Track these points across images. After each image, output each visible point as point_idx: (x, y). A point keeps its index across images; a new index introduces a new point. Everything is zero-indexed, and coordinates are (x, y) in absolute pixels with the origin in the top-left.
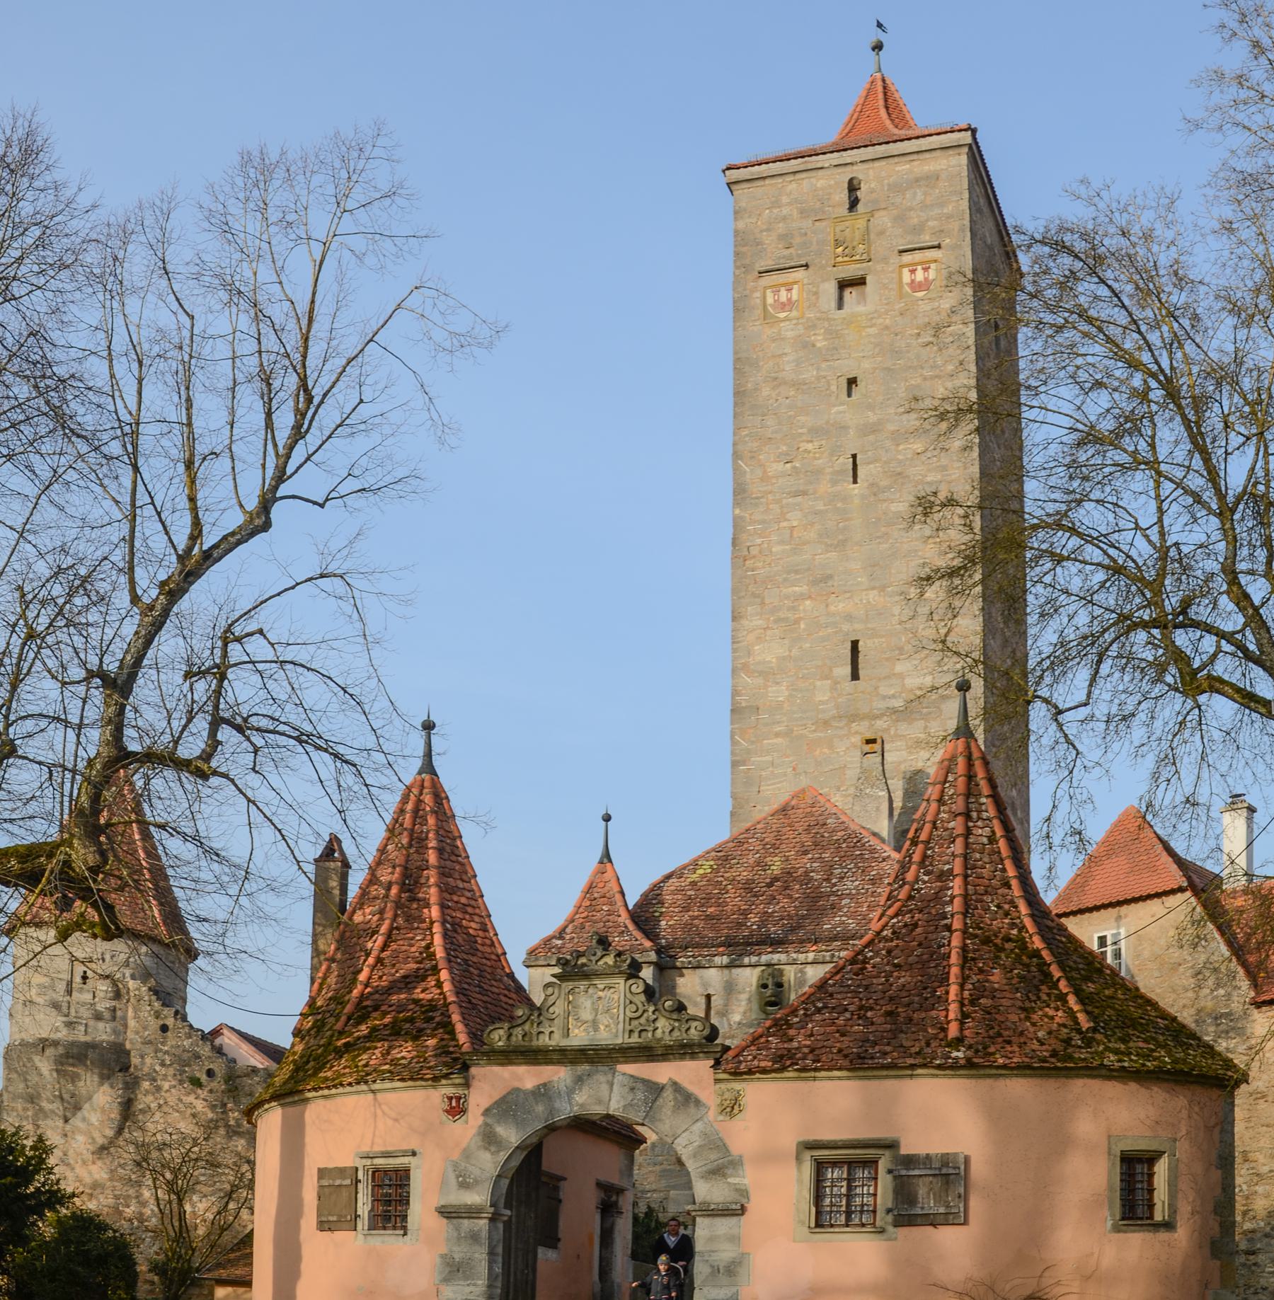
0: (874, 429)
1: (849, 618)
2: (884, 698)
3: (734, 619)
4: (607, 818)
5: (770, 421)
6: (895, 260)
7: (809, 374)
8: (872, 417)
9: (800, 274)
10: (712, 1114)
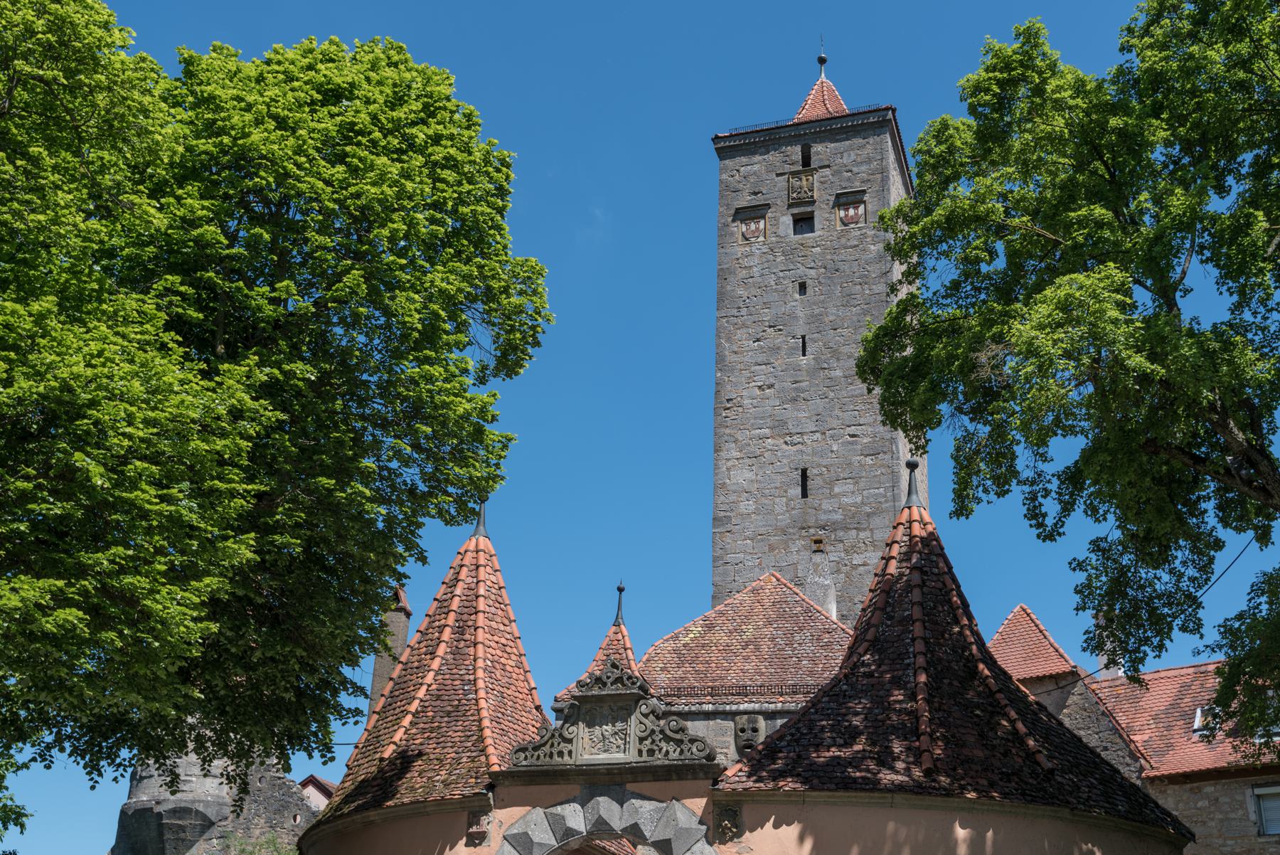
2: (825, 512)
3: (716, 451)
4: (621, 590)
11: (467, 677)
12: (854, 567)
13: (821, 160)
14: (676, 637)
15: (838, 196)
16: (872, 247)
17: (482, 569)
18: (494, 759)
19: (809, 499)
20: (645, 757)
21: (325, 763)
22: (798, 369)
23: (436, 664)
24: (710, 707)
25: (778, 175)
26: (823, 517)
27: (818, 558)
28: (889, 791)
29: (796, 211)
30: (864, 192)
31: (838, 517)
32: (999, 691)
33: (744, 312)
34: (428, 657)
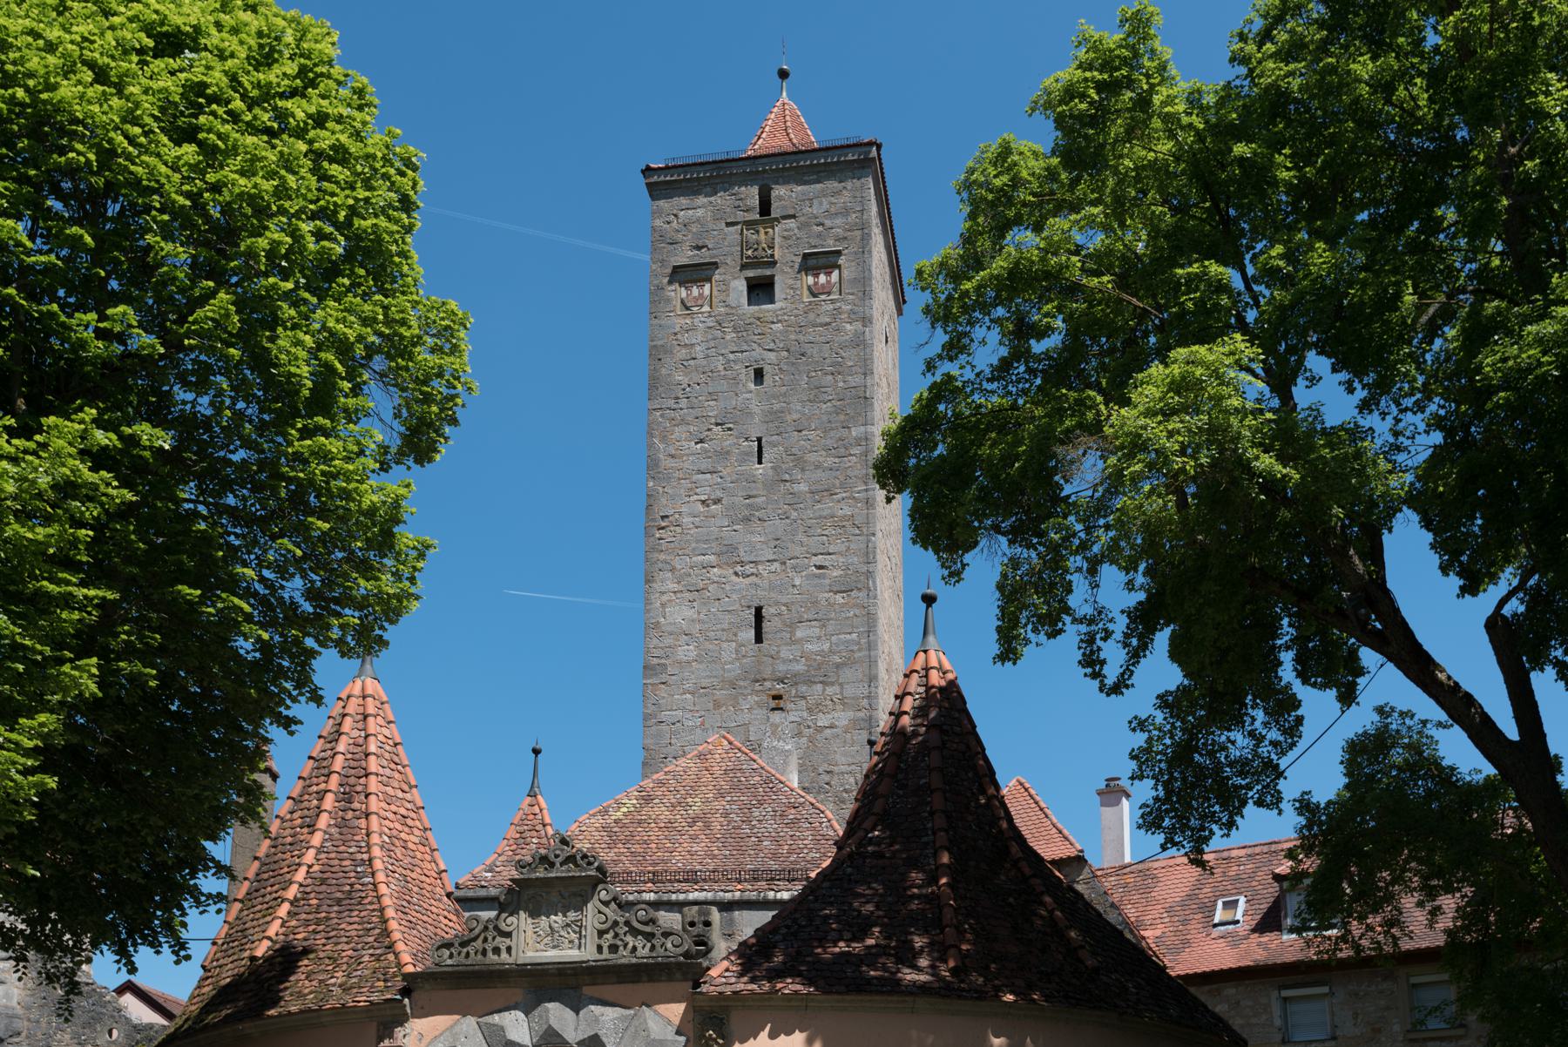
2: (784, 661)
11: (359, 856)
12: (820, 729)
13: (785, 207)
14: (605, 812)
15: (806, 256)
16: (848, 326)
17: (371, 719)
18: (406, 958)
19: (765, 645)
20: (606, 955)
21: (177, 962)
23: (317, 839)
25: (728, 225)
26: (782, 667)
27: (777, 717)
28: (911, 994)
29: (751, 273)
30: (839, 253)
31: (800, 667)
32: (1034, 876)
33: (683, 403)
34: (305, 830)
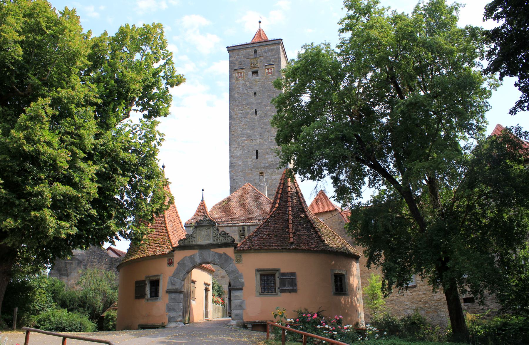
0: (260, 103)
1: (255, 145)
4: (203, 190)
5: (237, 102)
6: (264, 68)
7: (246, 92)
8: (260, 101)
9: (243, 70)
10: (234, 261)
22: (254, 119)
24: (231, 225)
31: (267, 165)
